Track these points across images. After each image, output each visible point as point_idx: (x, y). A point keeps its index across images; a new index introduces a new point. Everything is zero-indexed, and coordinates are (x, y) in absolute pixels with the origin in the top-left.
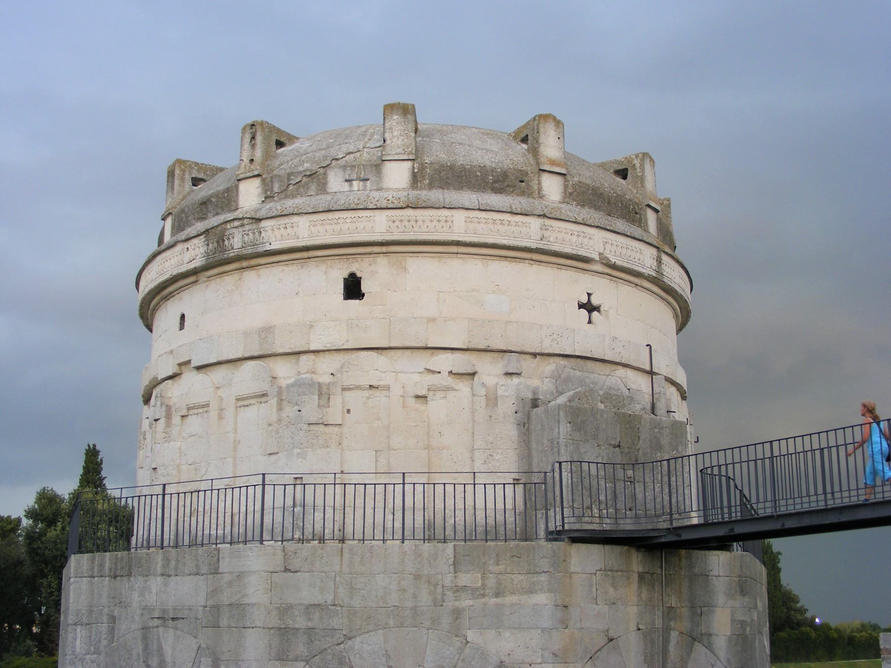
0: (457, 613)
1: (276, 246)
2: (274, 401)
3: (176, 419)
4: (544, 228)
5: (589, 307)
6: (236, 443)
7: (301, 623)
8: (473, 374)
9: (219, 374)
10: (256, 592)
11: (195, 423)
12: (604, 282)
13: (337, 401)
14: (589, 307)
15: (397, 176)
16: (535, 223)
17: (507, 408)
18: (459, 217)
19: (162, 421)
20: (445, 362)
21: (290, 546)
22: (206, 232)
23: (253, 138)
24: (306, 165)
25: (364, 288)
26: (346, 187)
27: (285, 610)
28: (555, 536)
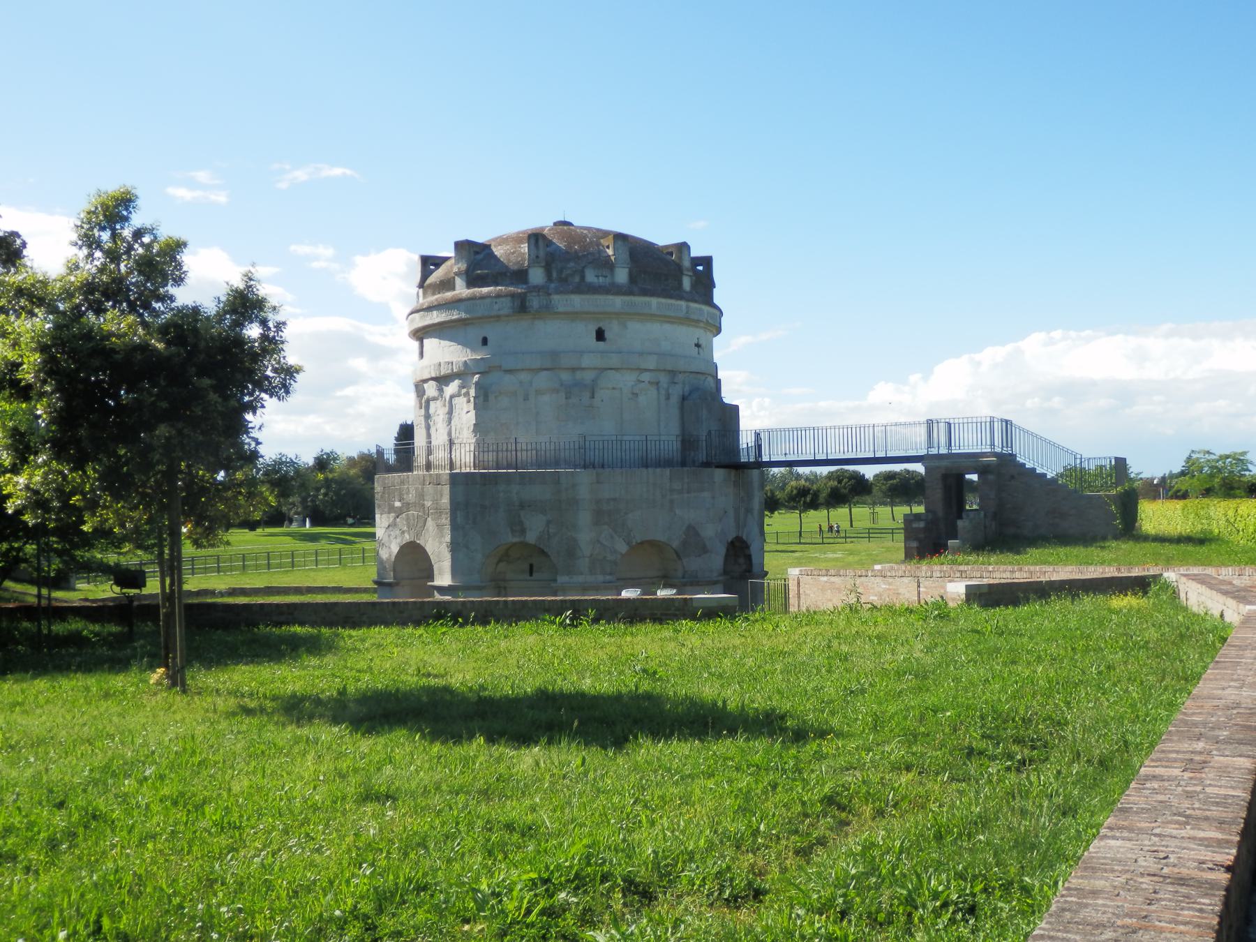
0: (672, 501)
1: (561, 309)
3: (491, 398)
4: (688, 307)
5: (698, 345)
8: (658, 383)
10: (584, 492)
12: (702, 331)
14: (698, 345)
15: (622, 276)
16: (683, 303)
17: (675, 400)
18: (654, 301)
19: (481, 398)
20: (646, 377)
21: (600, 470)
22: (513, 295)
25: (607, 335)
26: (595, 280)
28: (707, 465)
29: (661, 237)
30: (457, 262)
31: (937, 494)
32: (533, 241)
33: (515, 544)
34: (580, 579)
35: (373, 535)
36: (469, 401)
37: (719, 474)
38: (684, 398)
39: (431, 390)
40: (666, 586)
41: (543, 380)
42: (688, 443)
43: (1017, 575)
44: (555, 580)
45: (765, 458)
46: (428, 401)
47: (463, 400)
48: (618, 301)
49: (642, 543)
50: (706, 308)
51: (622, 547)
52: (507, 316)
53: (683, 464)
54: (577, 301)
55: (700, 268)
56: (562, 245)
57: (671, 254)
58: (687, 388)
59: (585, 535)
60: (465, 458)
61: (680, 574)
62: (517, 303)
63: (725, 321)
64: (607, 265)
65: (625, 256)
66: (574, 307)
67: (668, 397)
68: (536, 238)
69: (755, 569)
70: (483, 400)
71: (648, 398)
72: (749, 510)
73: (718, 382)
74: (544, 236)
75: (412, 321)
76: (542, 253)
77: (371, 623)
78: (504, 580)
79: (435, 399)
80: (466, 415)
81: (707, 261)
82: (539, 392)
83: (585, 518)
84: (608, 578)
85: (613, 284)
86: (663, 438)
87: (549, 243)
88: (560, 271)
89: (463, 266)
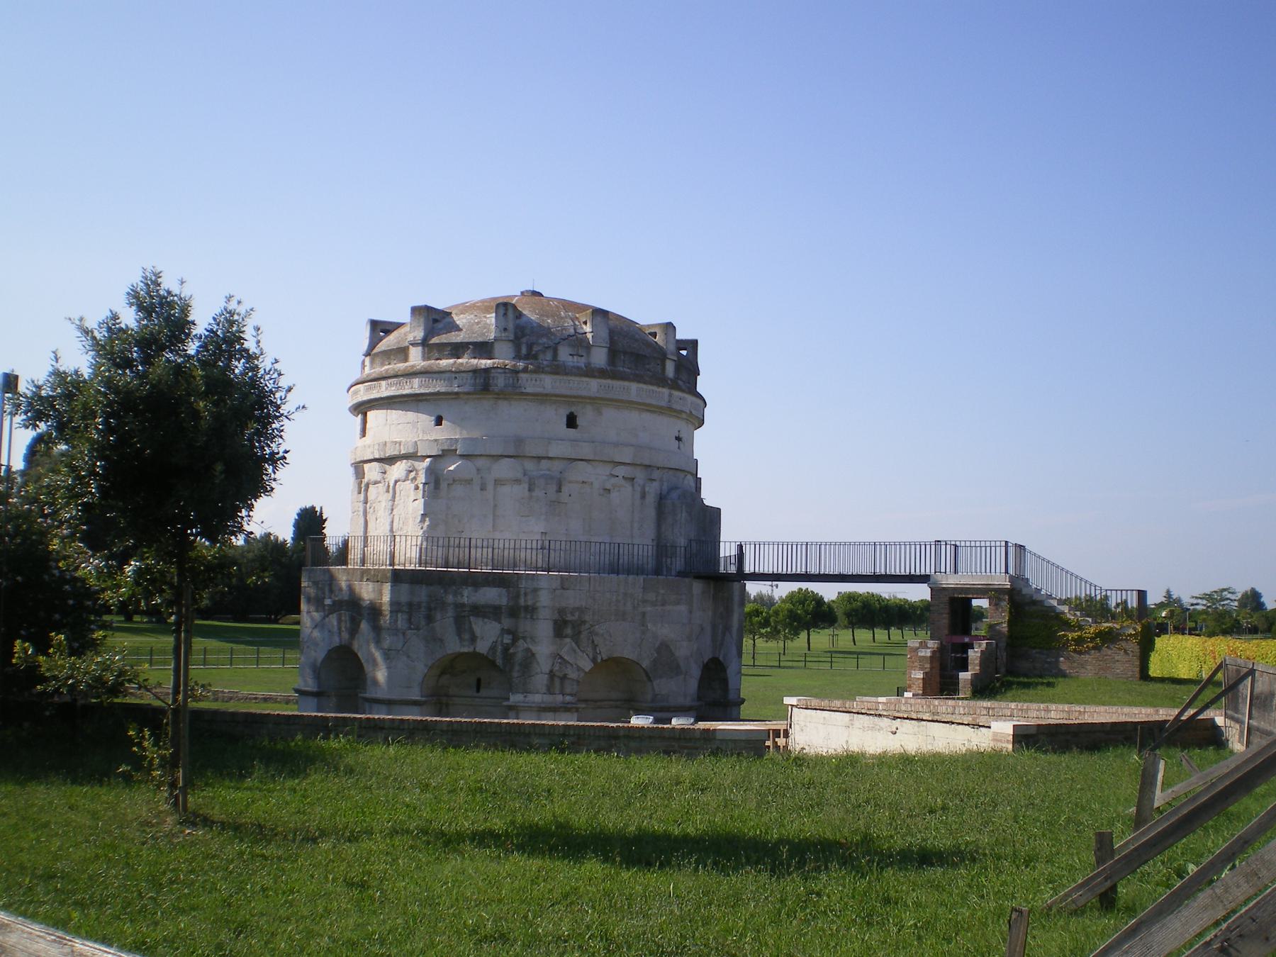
0: (644, 614)
1: (529, 390)
2: (526, 486)
3: (444, 485)
4: (670, 395)
5: (679, 439)
6: (495, 506)
7: (569, 618)
9: (481, 463)
10: (544, 599)
11: (459, 490)
13: (565, 489)
14: (679, 439)
15: (599, 358)
16: (666, 391)
17: (651, 499)
18: (634, 386)
19: (432, 485)
20: (621, 471)
22: (476, 371)
23: (505, 314)
24: (545, 340)
27: (561, 611)
28: (682, 574)
29: (643, 311)
30: (413, 329)
31: (944, 620)
32: (502, 311)
33: (463, 654)
34: (537, 698)
35: (297, 633)
36: (417, 488)
37: (697, 587)
38: (661, 498)
39: (372, 471)
40: (639, 712)
41: (505, 469)
42: (662, 549)
43: (1053, 714)
44: (508, 699)
45: (748, 568)
46: (367, 486)
47: (409, 486)
48: (593, 386)
49: (609, 659)
50: (690, 398)
51: (587, 665)
52: (468, 393)
53: (657, 571)
54: (548, 383)
55: (684, 352)
56: (534, 317)
57: (654, 335)
58: (665, 487)
59: (544, 647)
60: (409, 554)
61: (649, 697)
62: (480, 381)
63: (708, 412)
64: (578, 342)
65: (604, 334)
66: (572, 385)
67: (643, 496)
68: (504, 308)
69: (732, 696)
70: (435, 484)
71: (623, 497)
72: (727, 628)
73: (698, 481)
74: (514, 306)
75: (356, 393)
76: (511, 326)
77: (530, 748)
78: (447, 695)
79: (376, 483)
80: (411, 504)
81: (693, 345)
82: (498, 482)
83: (544, 628)
84: (568, 698)
85: (588, 365)
86: (636, 541)
87: (519, 315)
88: (530, 347)
89: (419, 334)
